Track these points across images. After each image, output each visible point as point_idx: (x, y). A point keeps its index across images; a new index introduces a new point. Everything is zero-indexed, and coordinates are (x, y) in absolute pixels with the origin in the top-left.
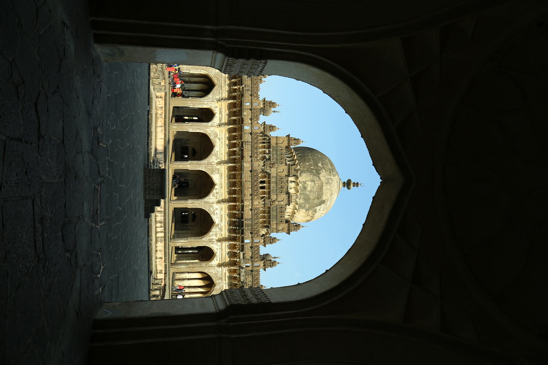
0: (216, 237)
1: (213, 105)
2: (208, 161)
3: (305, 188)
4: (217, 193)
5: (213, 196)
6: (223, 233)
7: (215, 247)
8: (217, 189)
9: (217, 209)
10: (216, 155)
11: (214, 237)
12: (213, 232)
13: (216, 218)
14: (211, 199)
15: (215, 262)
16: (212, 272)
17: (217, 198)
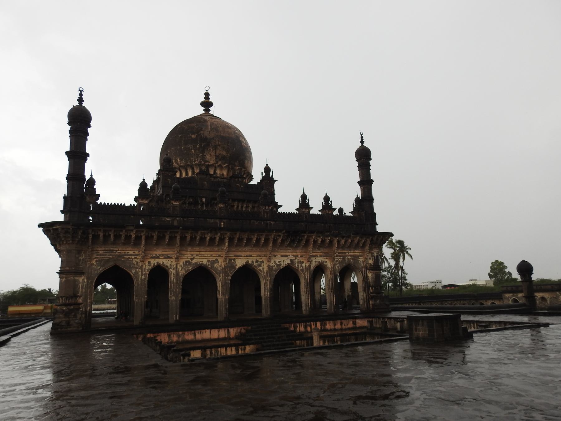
0: (303, 262)
1: (147, 268)
2: (220, 273)
3: (223, 158)
4: (257, 261)
5: (260, 266)
6: (299, 254)
7: (313, 265)
8: (253, 262)
9: (275, 262)
10: (213, 262)
11: (304, 265)
12: (298, 266)
13: (286, 262)
14: (263, 269)
15: (329, 264)
16: (338, 267)
17: (263, 262)
